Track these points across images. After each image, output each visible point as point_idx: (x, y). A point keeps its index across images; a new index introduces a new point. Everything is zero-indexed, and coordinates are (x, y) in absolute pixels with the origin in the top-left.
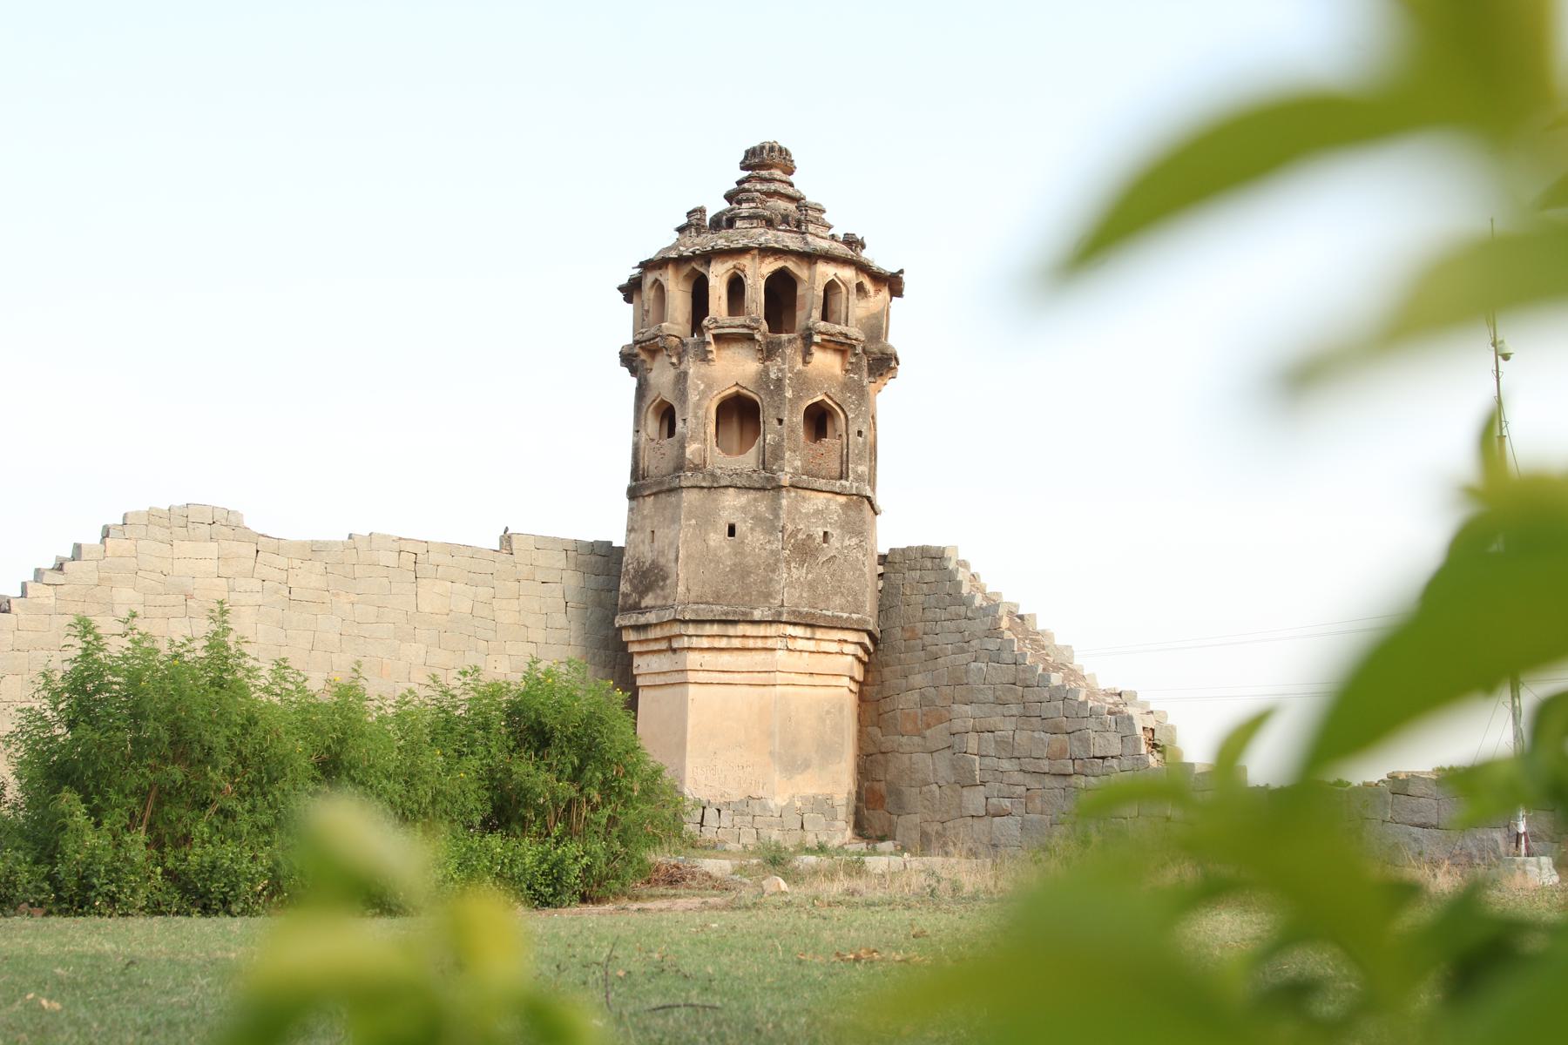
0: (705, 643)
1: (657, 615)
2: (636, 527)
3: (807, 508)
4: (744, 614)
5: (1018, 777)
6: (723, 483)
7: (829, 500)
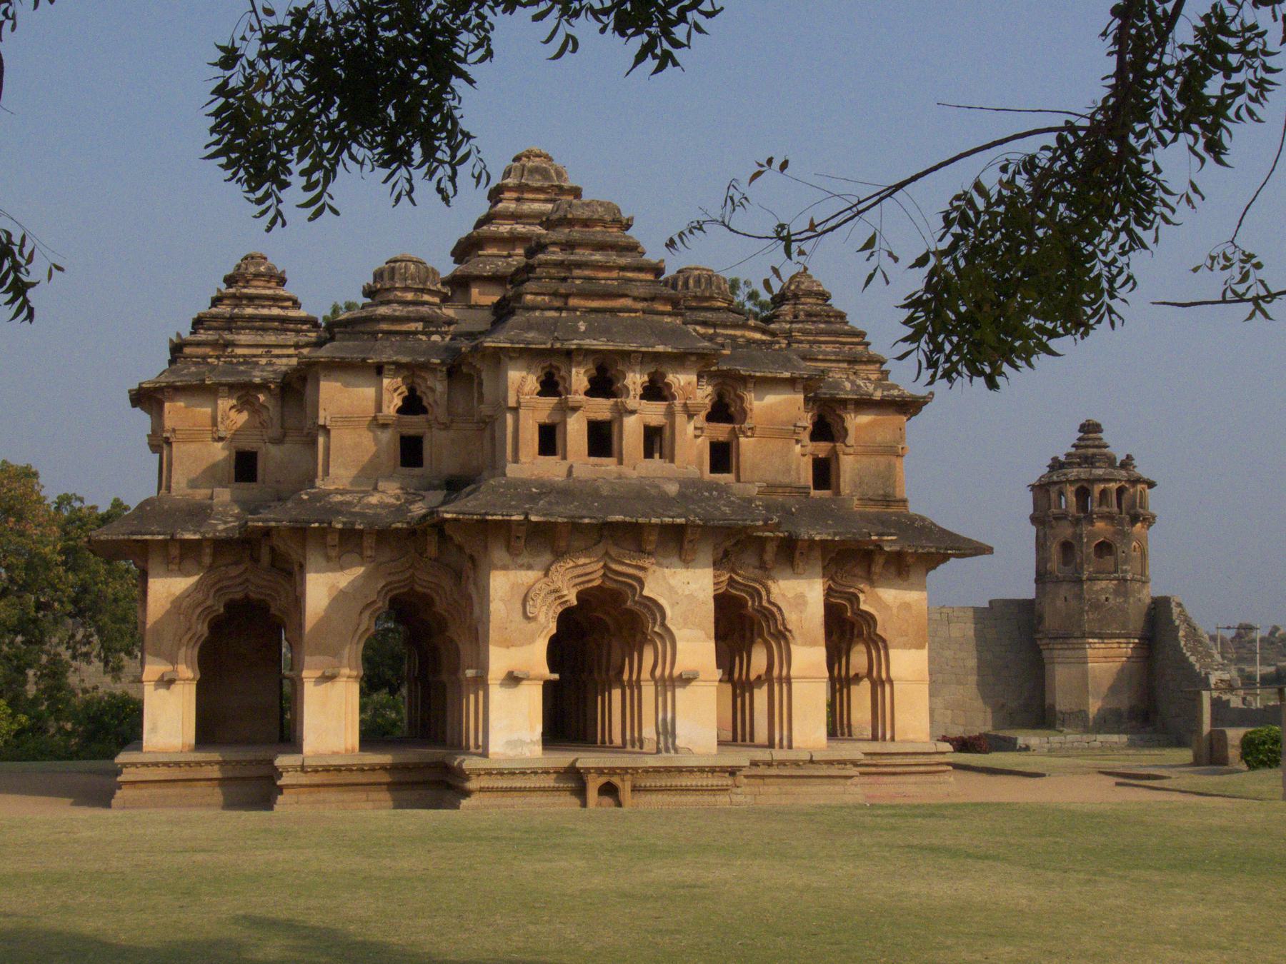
0: (1059, 647)
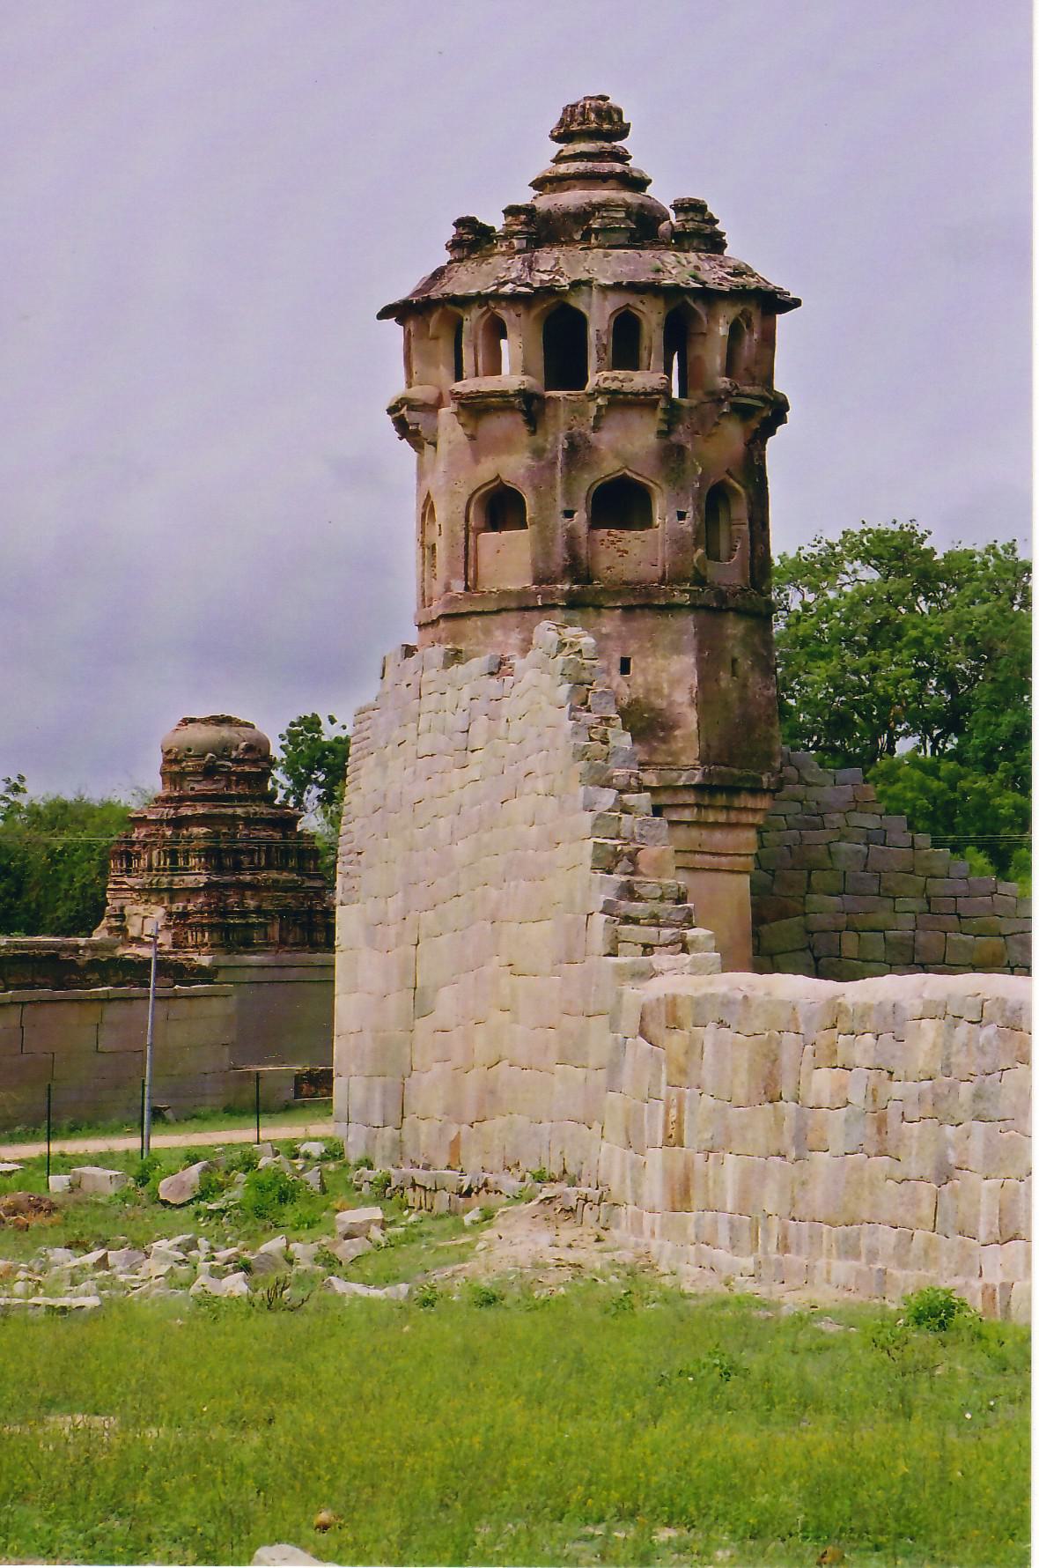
0: (711, 819)
1: (659, 778)
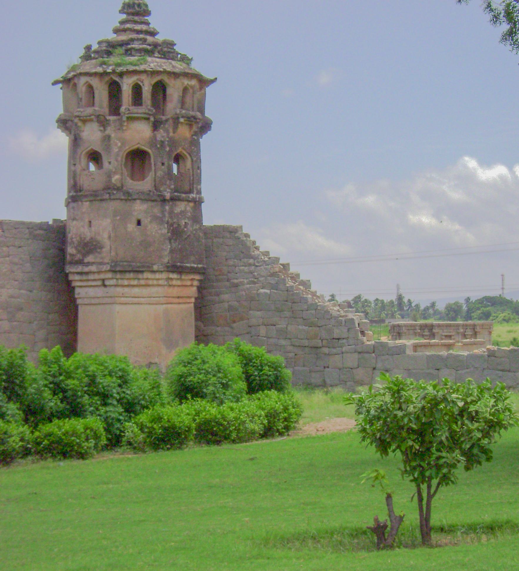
0: (126, 283)
2: (77, 218)
3: (177, 210)
4: (148, 267)
5: (290, 348)
6: (134, 197)
7: (186, 205)
